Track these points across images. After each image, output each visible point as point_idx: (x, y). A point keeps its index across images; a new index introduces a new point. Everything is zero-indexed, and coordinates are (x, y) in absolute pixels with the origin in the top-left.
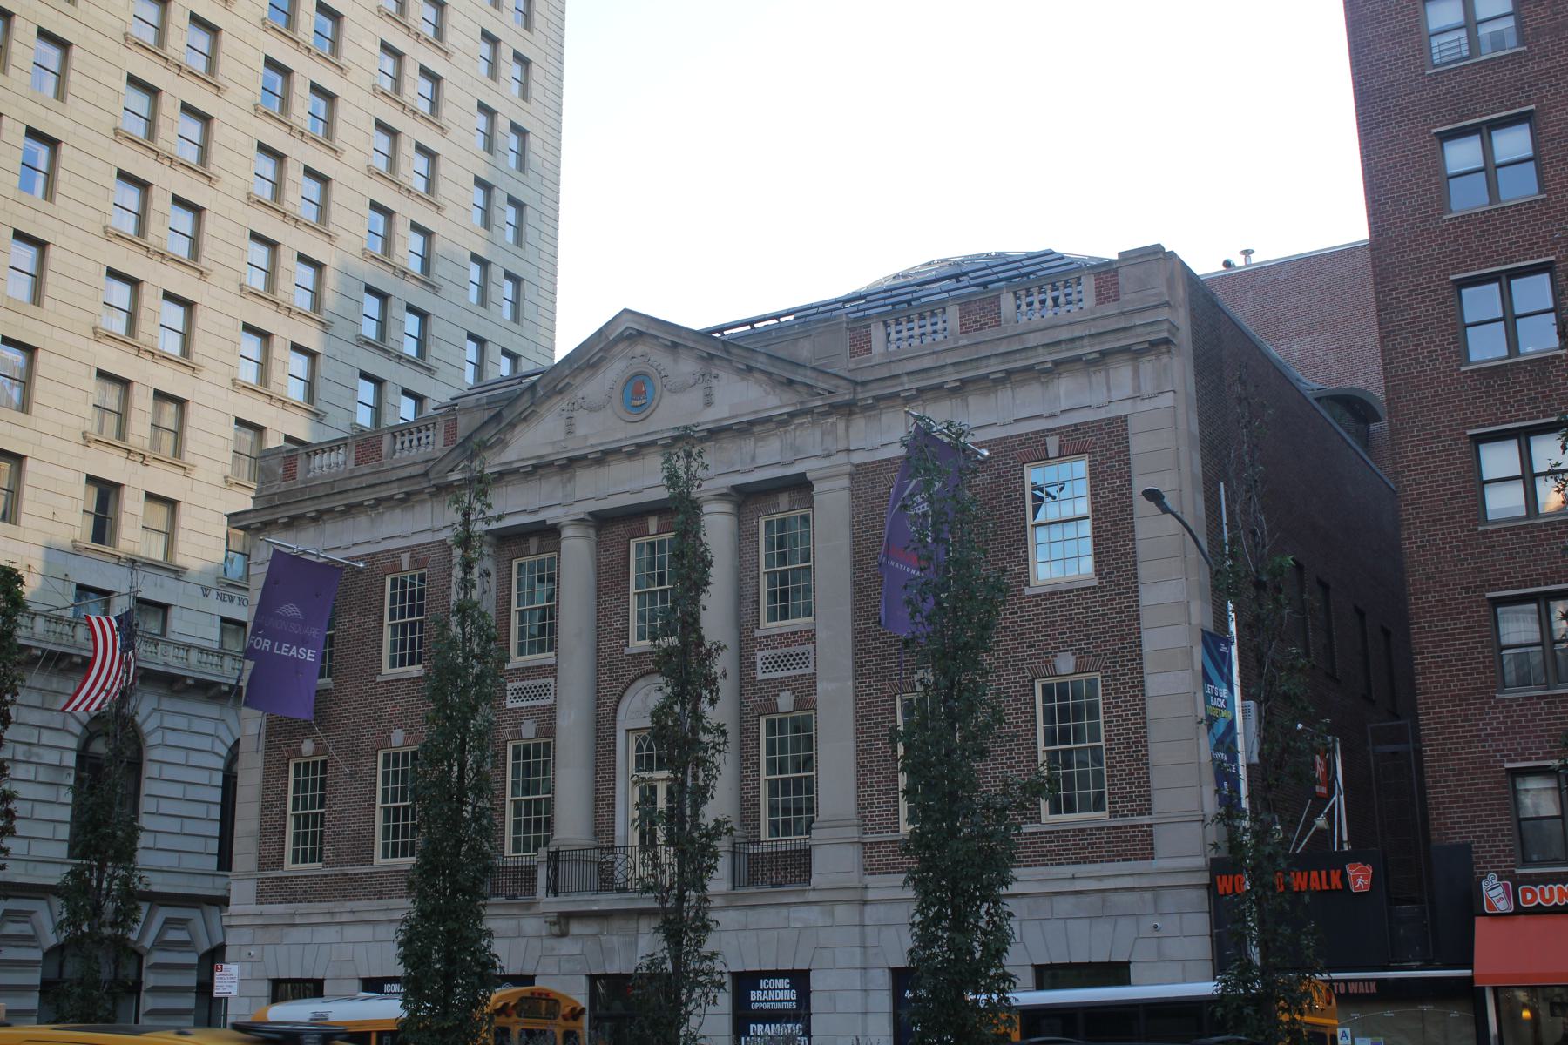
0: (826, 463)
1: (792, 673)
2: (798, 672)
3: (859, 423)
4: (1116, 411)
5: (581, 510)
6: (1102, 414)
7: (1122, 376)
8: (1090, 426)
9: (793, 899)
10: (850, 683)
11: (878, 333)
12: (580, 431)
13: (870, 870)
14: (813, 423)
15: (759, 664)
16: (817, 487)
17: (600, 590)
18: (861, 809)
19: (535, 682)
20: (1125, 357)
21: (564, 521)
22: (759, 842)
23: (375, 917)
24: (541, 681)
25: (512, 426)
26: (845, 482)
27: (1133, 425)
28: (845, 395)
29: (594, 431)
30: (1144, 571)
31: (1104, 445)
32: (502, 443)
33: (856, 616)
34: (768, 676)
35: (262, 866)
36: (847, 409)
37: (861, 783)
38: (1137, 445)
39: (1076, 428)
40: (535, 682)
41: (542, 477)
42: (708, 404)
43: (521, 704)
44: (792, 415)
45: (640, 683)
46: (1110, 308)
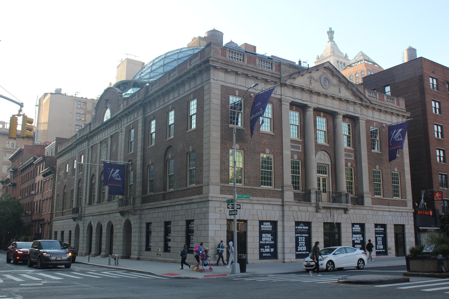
5: (316, 106)
12: (313, 85)
23: (265, 202)
24: (298, 145)
28: (368, 104)
29: (316, 87)
35: (222, 181)
46: (399, 107)
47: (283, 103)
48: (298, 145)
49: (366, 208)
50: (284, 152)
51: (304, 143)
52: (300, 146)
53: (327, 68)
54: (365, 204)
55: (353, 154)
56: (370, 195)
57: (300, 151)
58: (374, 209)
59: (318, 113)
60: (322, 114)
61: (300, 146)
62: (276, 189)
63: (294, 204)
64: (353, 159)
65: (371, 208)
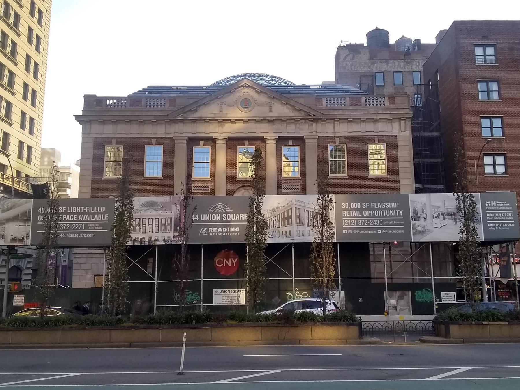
0: (310, 134)
3: (319, 125)
4: (394, 134)
5: (226, 136)
6: (390, 134)
7: (396, 125)
8: (387, 137)
11: (324, 101)
14: (305, 122)
20: (398, 120)
21: (220, 138)
25: (200, 106)
27: (399, 138)
30: (401, 175)
31: (390, 142)
32: (196, 111)
36: (316, 120)
38: (400, 143)
39: (383, 136)
40: (203, 185)
41: (211, 123)
42: (271, 111)
44: (300, 119)
53: (246, 86)
55: (300, 184)
57: (209, 191)
59: (240, 142)
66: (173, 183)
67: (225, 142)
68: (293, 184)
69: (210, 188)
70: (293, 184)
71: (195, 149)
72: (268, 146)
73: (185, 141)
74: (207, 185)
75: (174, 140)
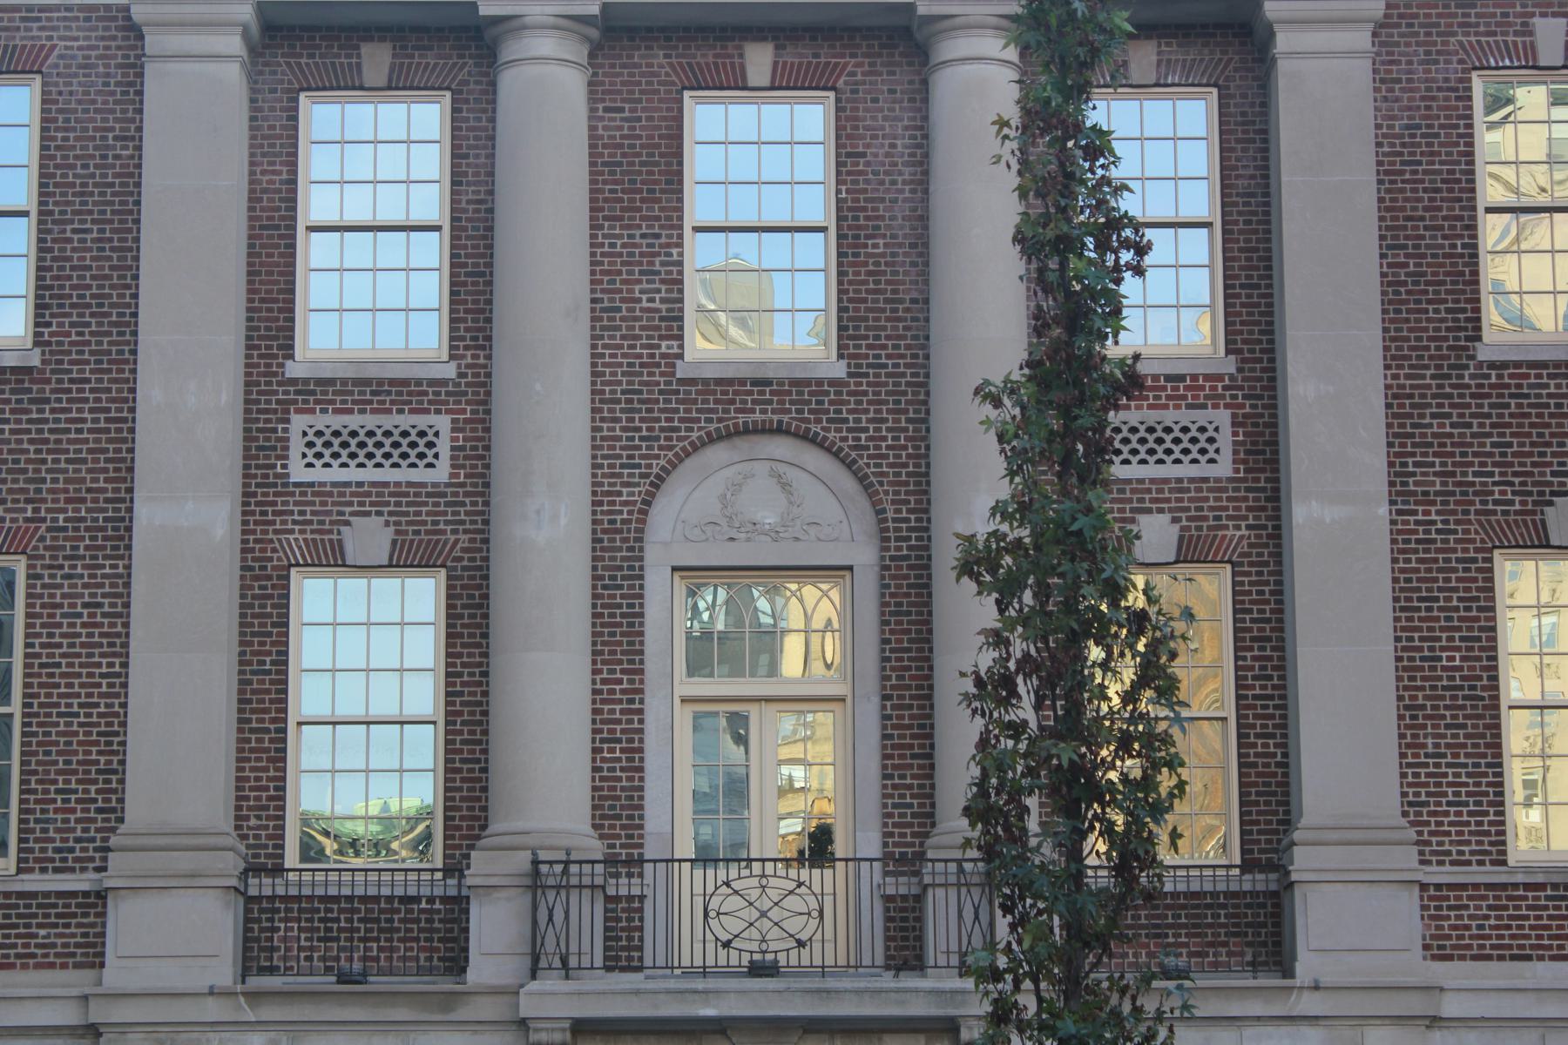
1: (388, 475)
2: (1186, 470)
9: (1255, 1008)
10: (1383, 510)
13: (1437, 950)
15: (296, 446)
16: (1284, 41)
17: (601, 210)
18: (1410, 806)
19: (388, 422)
21: (535, 12)
22: (279, 870)
24: (405, 421)
26: (1362, 39)
33: (1392, 360)
34: (318, 474)
37: (1409, 745)
40: (388, 422)
43: (336, 474)
45: (717, 454)
47: (153, 42)
48: (405, 421)
49: (1309, 1004)
50: (148, 514)
51: (484, 401)
52: (443, 423)
54: (1307, 965)
55: (1223, 417)
56: (1407, 858)
57: (441, 473)
58: (1451, 1007)
59: (704, 56)
60: (759, 60)
61: (443, 423)
62: (35, 882)
63: (214, 1010)
64: (1224, 468)
65: (1415, 1005)
66: (128, 400)
67: (580, 53)
68: (1169, 416)
69: (444, 447)
70: (1169, 416)
71: (322, 117)
72: (949, 85)
73: (233, 44)
74: (422, 421)
75: (134, 32)
